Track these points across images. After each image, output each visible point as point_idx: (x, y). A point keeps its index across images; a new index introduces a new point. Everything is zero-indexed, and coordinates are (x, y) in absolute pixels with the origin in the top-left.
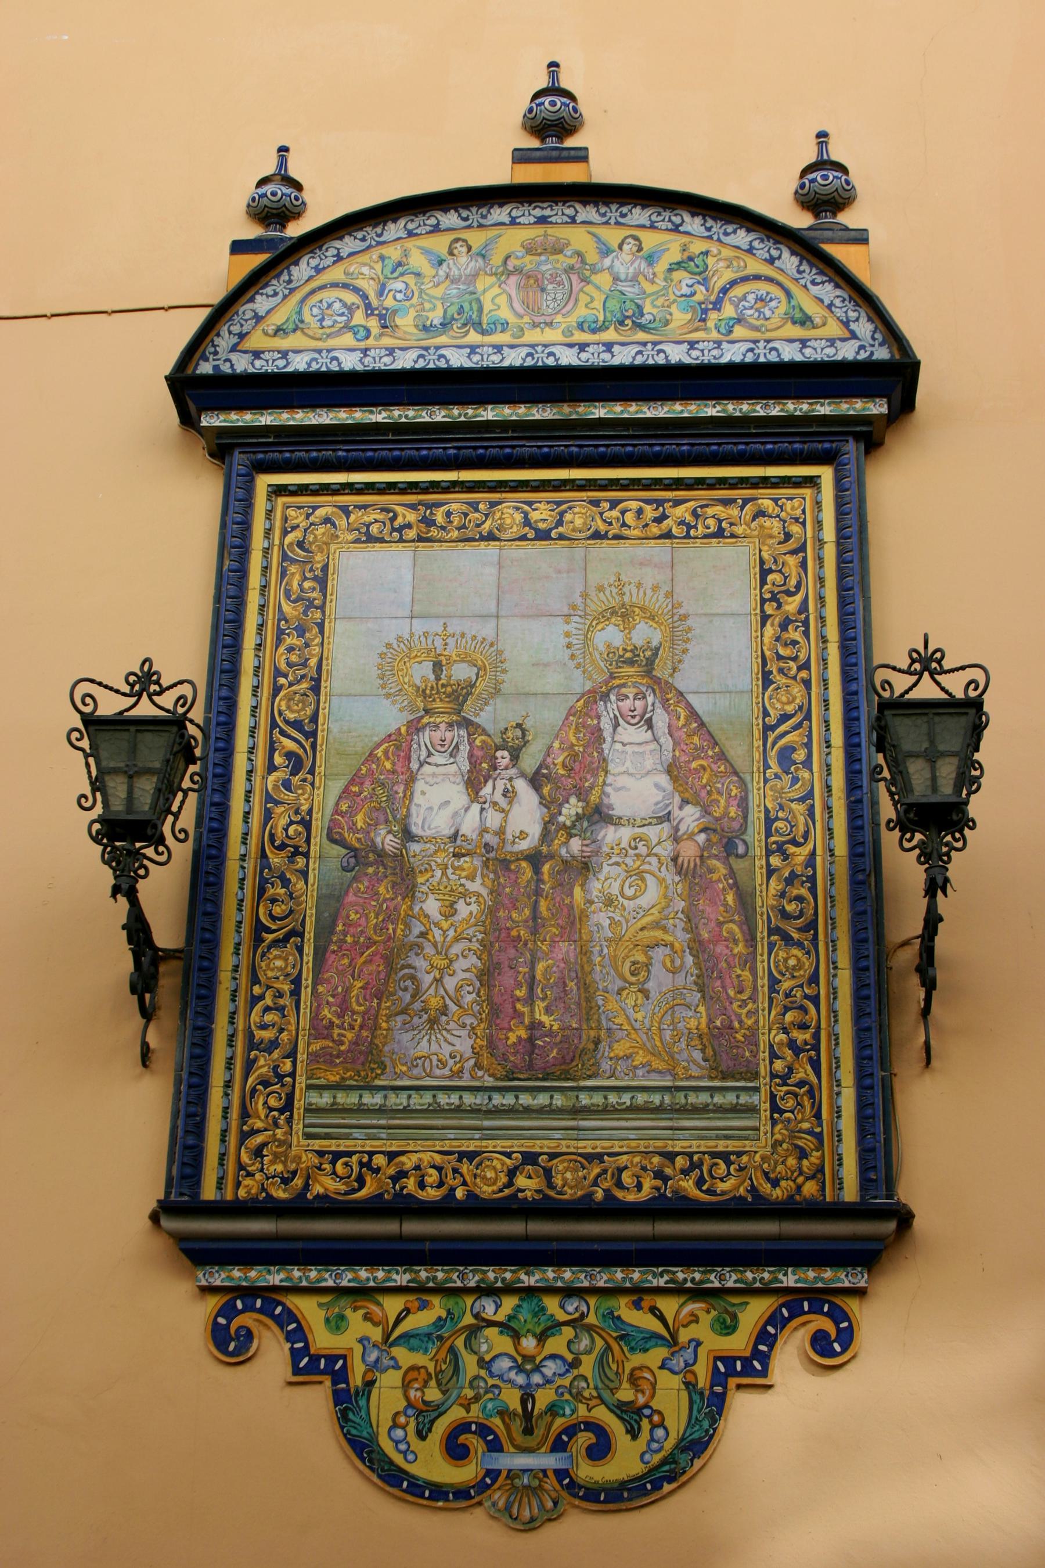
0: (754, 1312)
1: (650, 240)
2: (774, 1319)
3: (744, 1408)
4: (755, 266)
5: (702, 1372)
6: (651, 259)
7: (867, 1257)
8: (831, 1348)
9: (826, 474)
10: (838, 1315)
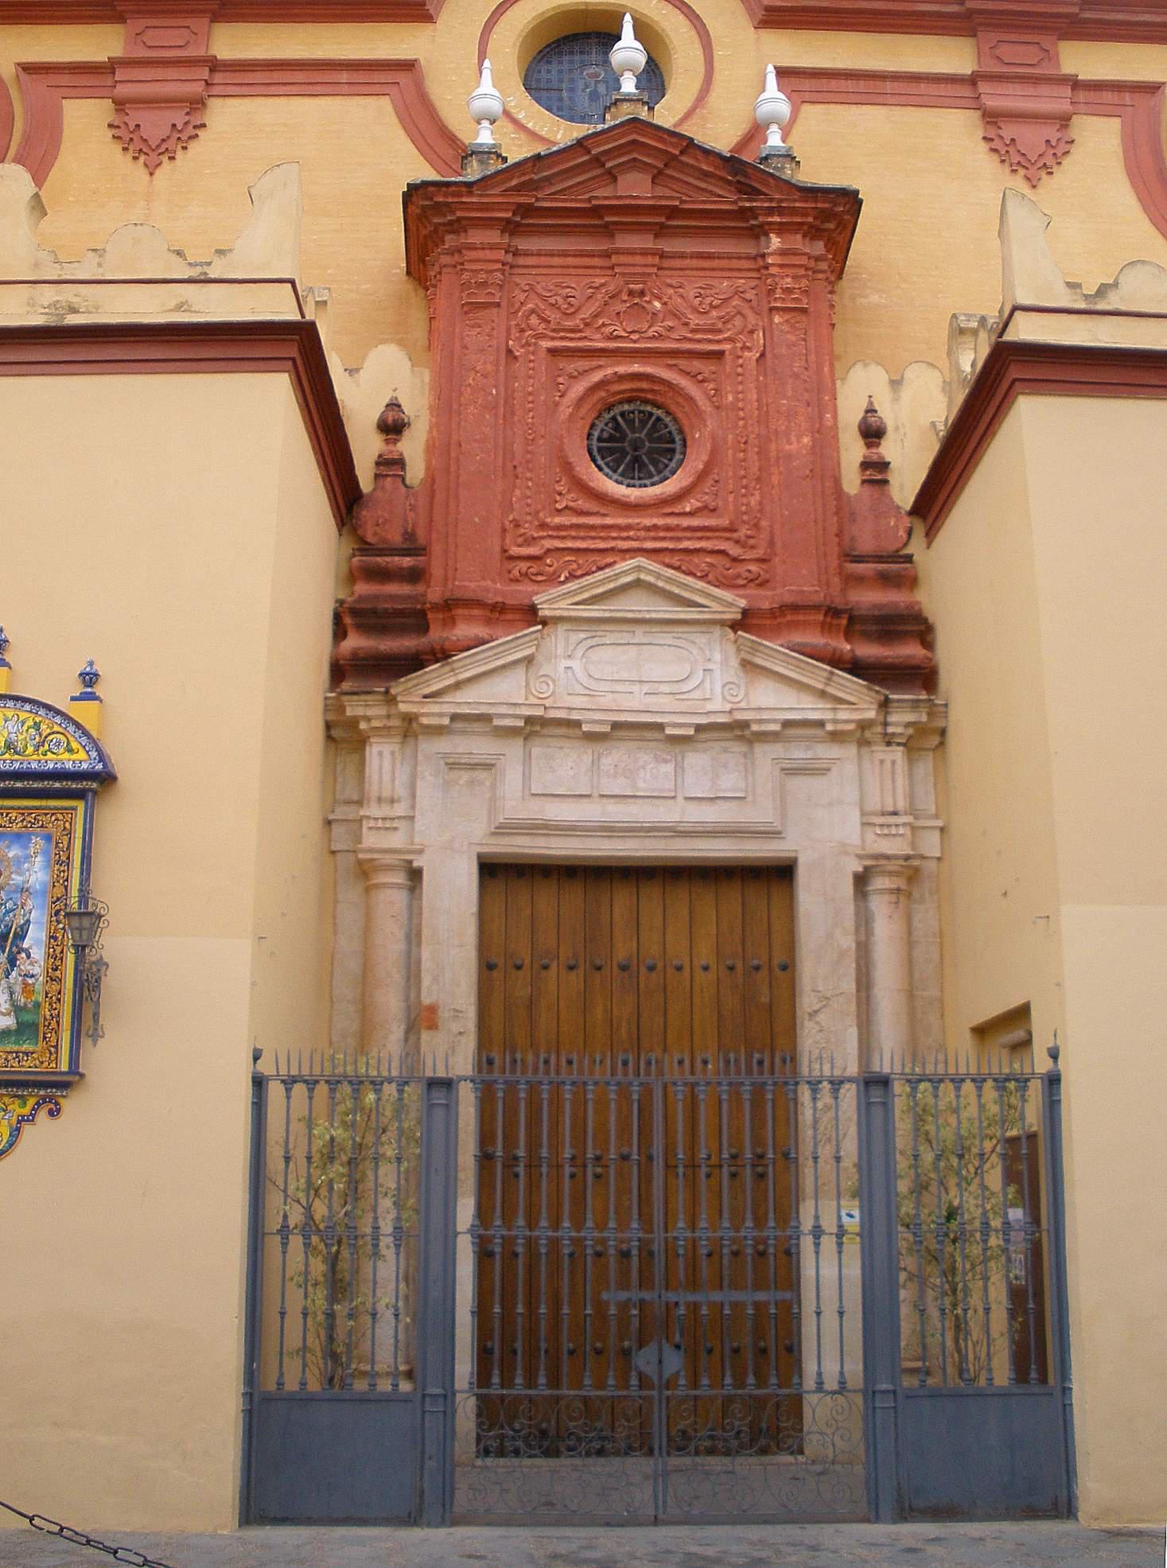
0: (31, 1102)
1: (23, 716)
2: (38, 1103)
3: (27, 1129)
4: (56, 728)
5: (14, 1119)
6: (23, 723)
7: (65, 1086)
8: (54, 1113)
9: (80, 805)
10: (57, 1104)
